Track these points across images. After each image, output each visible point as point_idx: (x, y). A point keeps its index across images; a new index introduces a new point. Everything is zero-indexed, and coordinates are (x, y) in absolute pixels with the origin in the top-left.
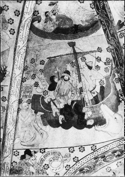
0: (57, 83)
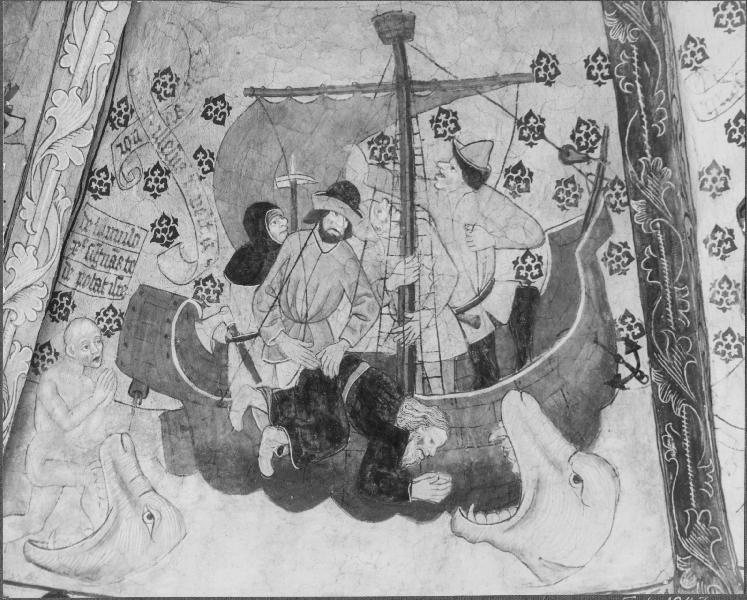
0: (278, 247)
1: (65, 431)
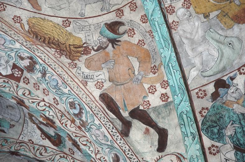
1: (193, 39)
